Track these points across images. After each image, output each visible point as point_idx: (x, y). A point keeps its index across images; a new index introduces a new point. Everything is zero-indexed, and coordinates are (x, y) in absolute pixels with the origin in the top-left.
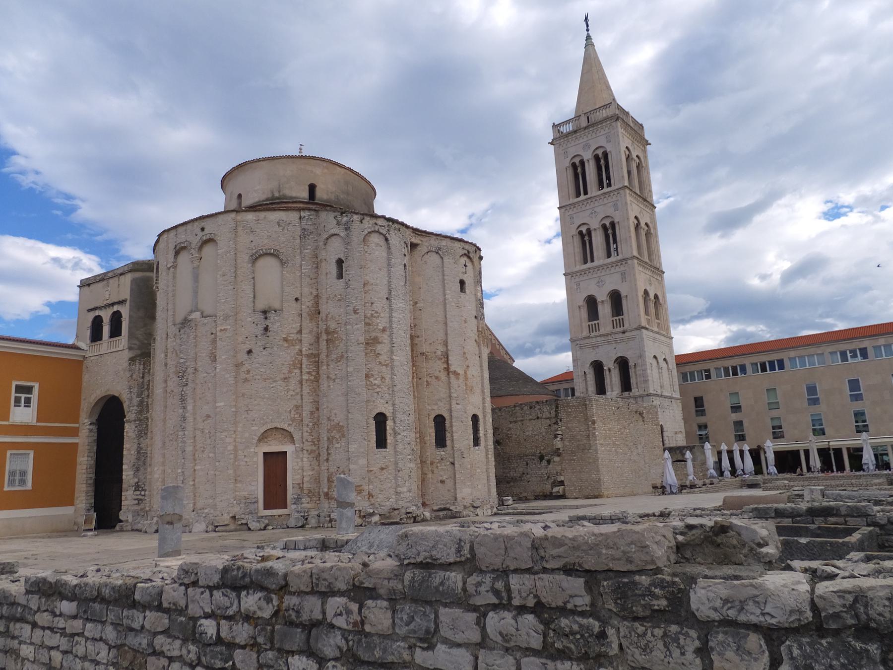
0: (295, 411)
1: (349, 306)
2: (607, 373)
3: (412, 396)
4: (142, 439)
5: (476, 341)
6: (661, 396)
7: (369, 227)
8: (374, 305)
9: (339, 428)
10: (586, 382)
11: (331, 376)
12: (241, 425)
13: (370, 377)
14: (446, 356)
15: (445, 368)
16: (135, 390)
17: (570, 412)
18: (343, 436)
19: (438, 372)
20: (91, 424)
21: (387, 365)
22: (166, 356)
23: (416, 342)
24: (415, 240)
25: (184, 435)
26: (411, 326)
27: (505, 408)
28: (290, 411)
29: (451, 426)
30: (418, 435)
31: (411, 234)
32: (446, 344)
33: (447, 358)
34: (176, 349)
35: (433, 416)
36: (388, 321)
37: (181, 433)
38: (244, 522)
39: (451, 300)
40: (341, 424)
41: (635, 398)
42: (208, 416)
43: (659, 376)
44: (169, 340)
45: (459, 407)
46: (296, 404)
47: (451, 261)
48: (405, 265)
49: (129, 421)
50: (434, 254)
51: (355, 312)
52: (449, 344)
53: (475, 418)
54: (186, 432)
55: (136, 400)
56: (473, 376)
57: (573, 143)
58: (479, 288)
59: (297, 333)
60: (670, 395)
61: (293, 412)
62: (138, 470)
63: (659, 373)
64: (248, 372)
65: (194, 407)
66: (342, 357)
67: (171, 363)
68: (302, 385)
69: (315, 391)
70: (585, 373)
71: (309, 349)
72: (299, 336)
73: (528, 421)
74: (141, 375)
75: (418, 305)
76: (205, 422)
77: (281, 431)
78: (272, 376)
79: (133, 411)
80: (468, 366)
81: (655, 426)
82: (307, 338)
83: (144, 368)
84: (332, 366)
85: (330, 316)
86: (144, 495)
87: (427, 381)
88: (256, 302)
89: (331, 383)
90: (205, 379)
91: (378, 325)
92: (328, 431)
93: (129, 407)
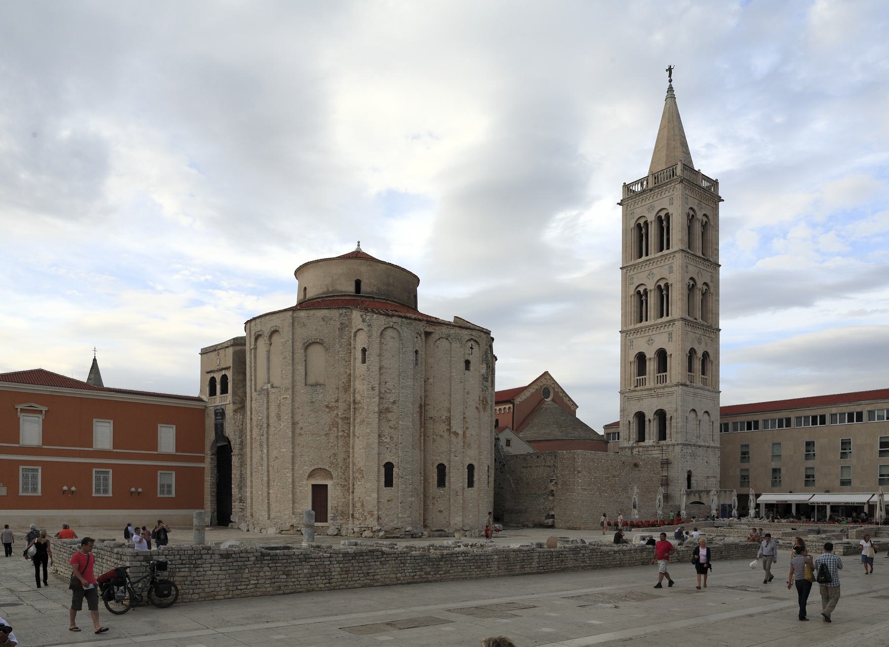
0: (333, 457)
1: (369, 384)
2: (647, 423)
3: (419, 451)
5: (477, 408)
6: (694, 445)
7: (385, 324)
8: (387, 384)
9: (361, 471)
10: (629, 430)
11: (356, 434)
12: (297, 465)
13: (382, 437)
14: (449, 419)
15: (448, 429)
16: (237, 433)
17: (564, 463)
19: (442, 432)
20: (211, 455)
21: (395, 428)
22: (251, 413)
23: (427, 409)
24: (428, 329)
25: (262, 469)
26: (421, 397)
27: (519, 456)
28: (330, 457)
29: (449, 473)
30: (422, 478)
31: (425, 325)
32: (449, 411)
33: (450, 421)
35: (436, 465)
36: (398, 396)
37: (260, 468)
39: (456, 377)
40: (362, 468)
41: (668, 446)
43: (697, 428)
45: (456, 458)
46: (334, 452)
47: (458, 345)
48: (416, 352)
50: (445, 340)
51: (373, 389)
52: (451, 411)
53: (471, 468)
54: (263, 468)
55: (238, 441)
56: (472, 435)
58: (484, 366)
59: (336, 402)
60: (707, 444)
61: (332, 458)
63: (697, 424)
64: (302, 428)
65: (268, 451)
66: (363, 421)
67: (254, 419)
68: (338, 439)
69: (348, 443)
70: (629, 422)
71: (344, 414)
72: (336, 404)
73: (534, 468)
75: (429, 381)
77: (324, 471)
78: (317, 432)
79: (237, 448)
80: (467, 428)
81: (654, 475)
82: (342, 406)
83: (243, 418)
85: (357, 390)
87: (433, 439)
88: (307, 378)
90: (275, 432)
91: (389, 399)
92: (353, 472)
93: (234, 445)
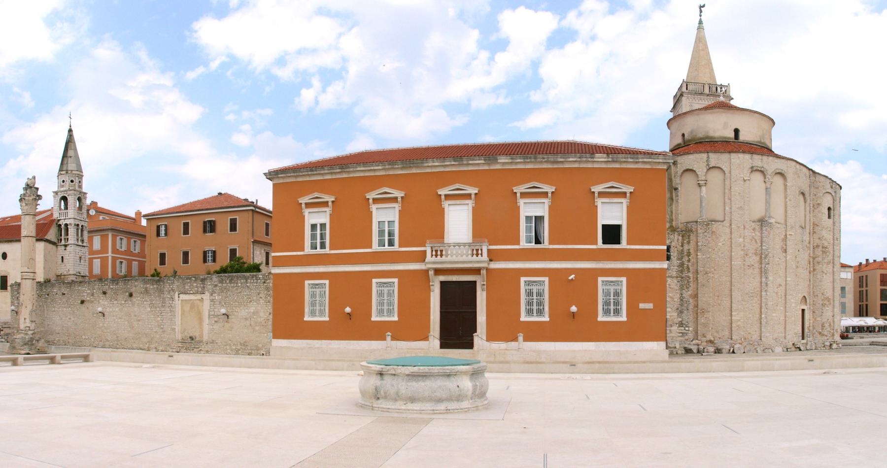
4: (684, 291)
9: (828, 299)
11: (824, 271)
18: (830, 304)
25: (767, 294)
34: (756, 238)
38: (798, 346)
42: (780, 285)
44: (746, 231)
49: (671, 277)
54: (768, 293)
57: (697, 101)
62: (681, 312)
74: (680, 244)
76: (779, 288)
79: (674, 270)
83: (683, 240)
84: (825, 266)
86: (689, 330)
89: (824, 275)
92: (822, 300)
